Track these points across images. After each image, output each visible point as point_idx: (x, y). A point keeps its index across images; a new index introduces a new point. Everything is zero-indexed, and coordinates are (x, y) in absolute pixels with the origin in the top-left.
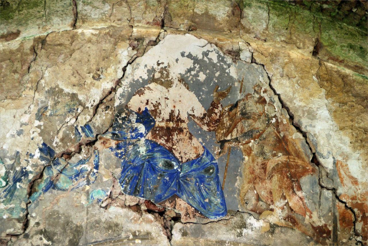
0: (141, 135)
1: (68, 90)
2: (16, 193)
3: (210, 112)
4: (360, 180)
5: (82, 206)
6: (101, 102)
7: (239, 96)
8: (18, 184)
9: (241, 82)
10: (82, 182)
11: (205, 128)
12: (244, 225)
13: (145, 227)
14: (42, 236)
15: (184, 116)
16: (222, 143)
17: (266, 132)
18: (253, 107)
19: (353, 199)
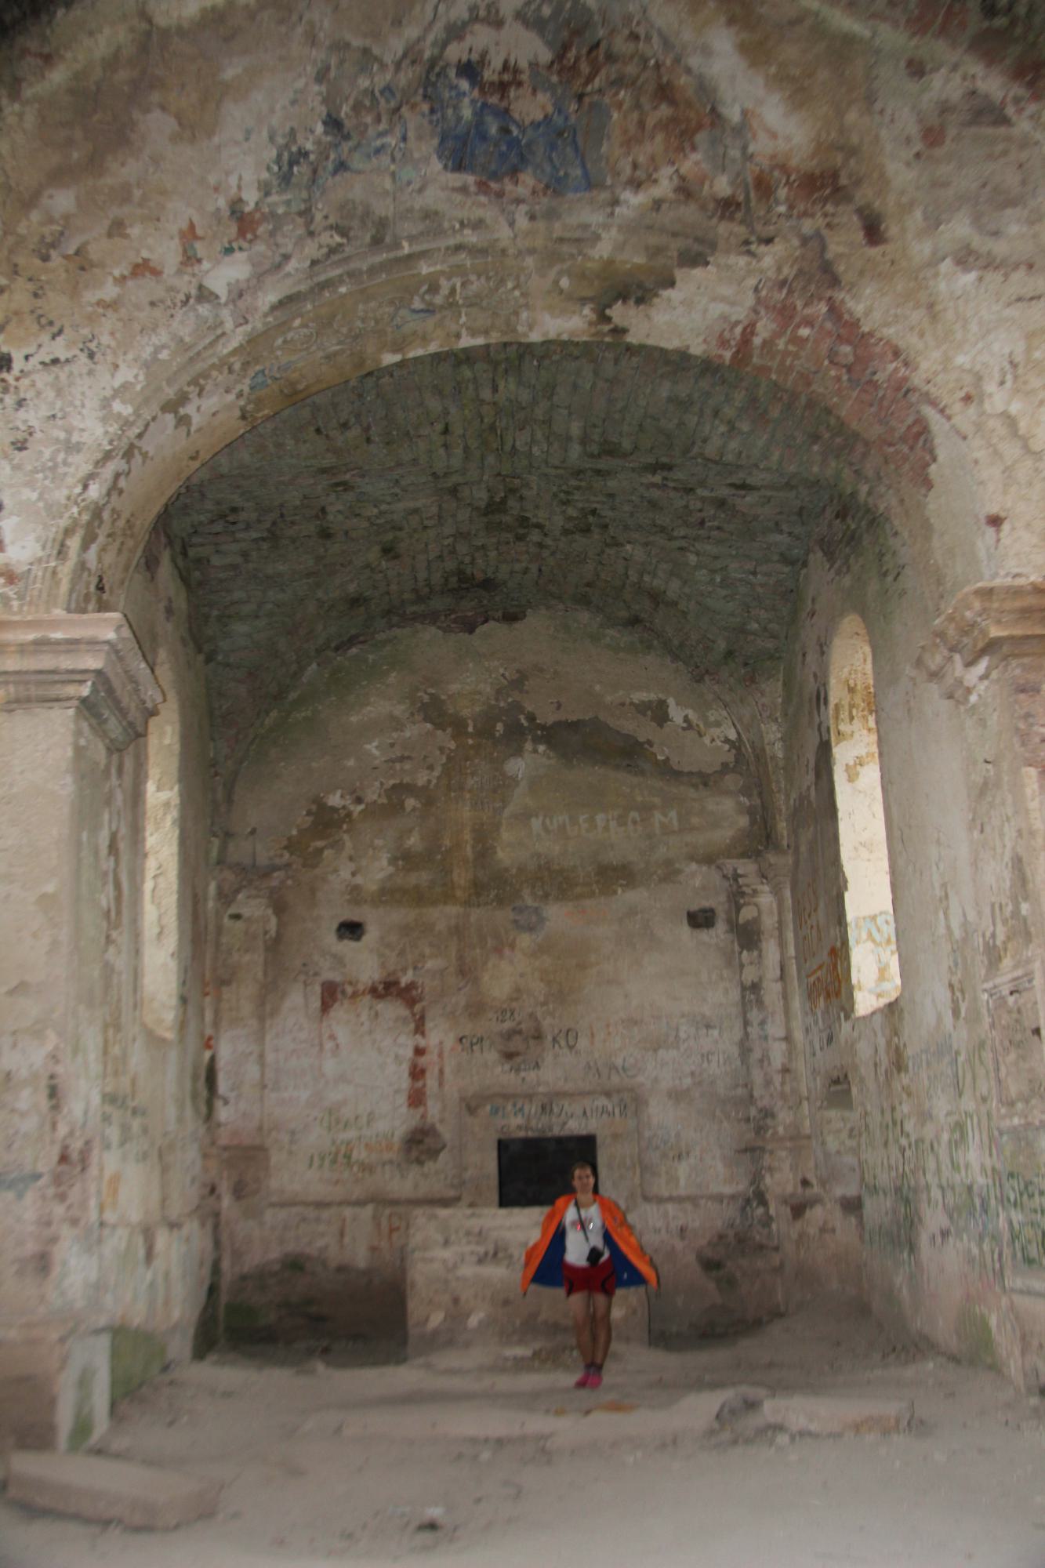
0: (464, 94)
1: (357, 42)
2: (294, 180)
3: (560, 56)
5: (386, 193)
6: (405, 55)
7: (601, 33)
8: (295, 169)
10: (385, 159)
12: (615, 202)
13: (479, 213)
14: (334, 233)
15: (523, 64)
16: (580, 97)
17: (641, 80)
18: (620, 45)
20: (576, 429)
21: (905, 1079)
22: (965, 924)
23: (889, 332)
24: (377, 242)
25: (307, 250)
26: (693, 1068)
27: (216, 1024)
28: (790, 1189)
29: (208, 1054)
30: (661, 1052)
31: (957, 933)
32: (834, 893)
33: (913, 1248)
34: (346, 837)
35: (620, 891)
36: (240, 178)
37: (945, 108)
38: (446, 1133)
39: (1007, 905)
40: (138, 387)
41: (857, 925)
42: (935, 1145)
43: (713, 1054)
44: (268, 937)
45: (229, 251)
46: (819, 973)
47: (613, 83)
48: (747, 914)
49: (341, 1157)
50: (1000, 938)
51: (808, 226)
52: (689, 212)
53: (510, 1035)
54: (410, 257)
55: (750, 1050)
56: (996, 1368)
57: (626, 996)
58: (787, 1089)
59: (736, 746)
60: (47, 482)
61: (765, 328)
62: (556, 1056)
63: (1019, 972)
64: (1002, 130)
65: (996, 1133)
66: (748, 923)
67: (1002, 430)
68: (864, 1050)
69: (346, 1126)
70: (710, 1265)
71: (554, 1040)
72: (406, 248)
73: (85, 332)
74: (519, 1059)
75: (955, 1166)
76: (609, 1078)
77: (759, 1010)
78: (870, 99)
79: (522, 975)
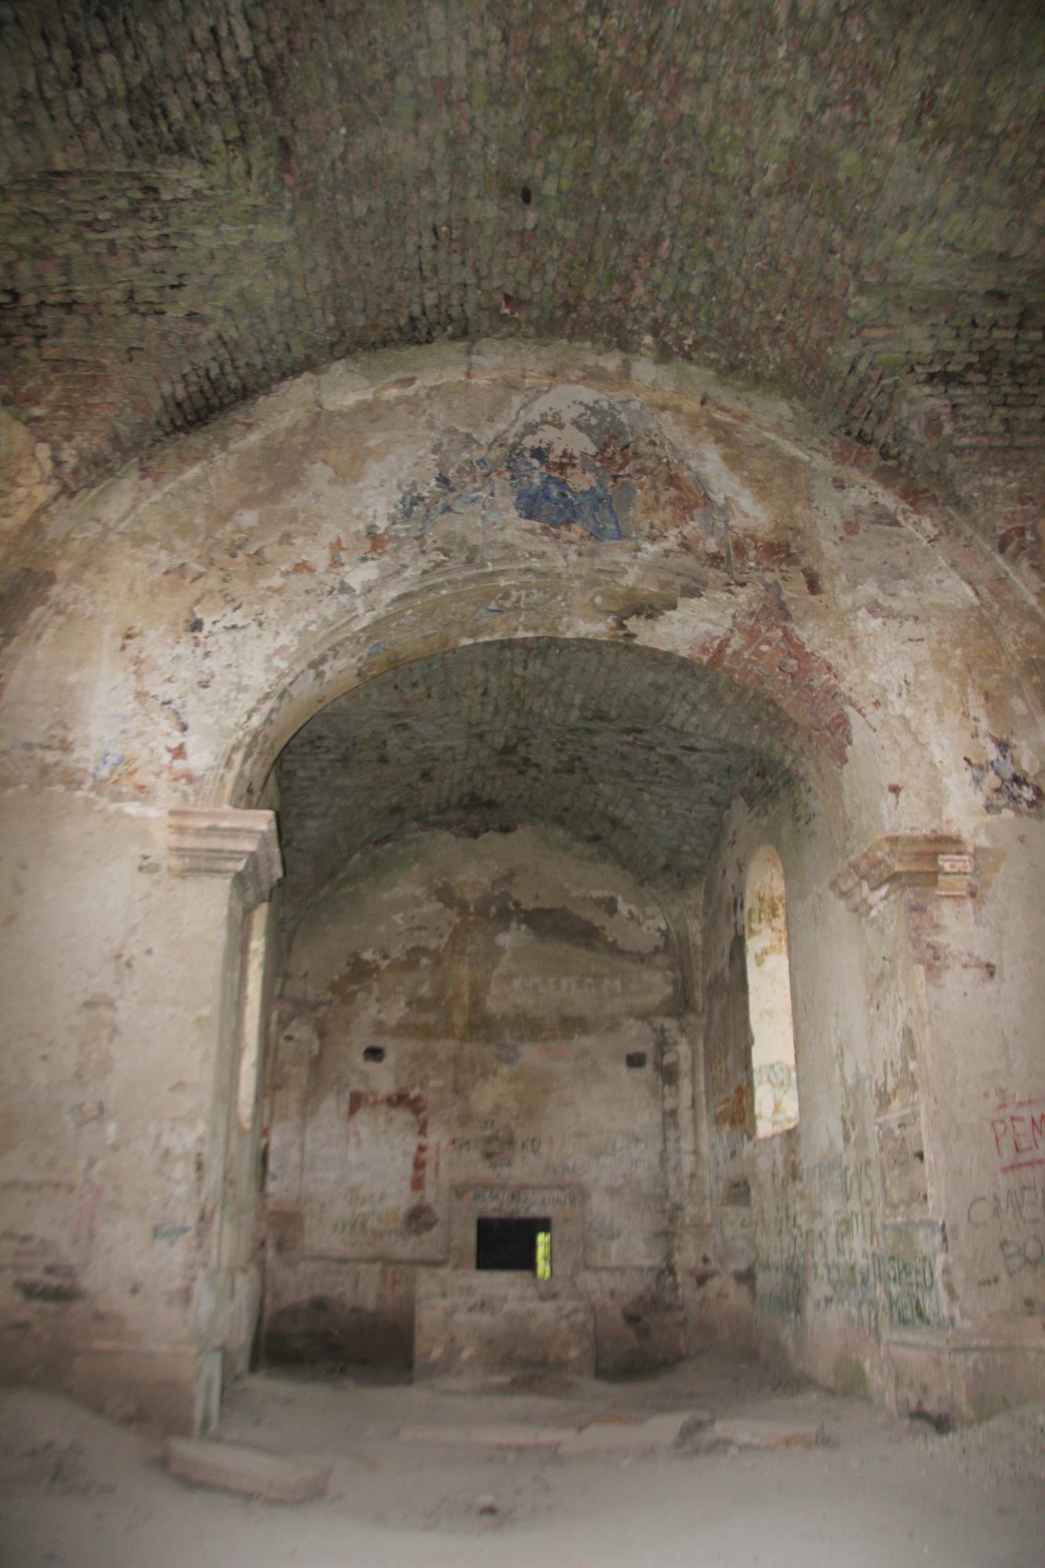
0: (535, 468)
1: (462, 430)
2: (413, 515)
3: (602, 451)
4: (751, 515)
6: (495, 441)
7: (630, 438)
9: (632, 427)
10: (478, 507)
11: (598, 464)
12: (638, 549)
13: (543, 548)
15: (577, 453)
16: (615, 478)
18: (644, 448)
19: (745, 530)
20: (578, 699)
21: (799, 1186)
22: (857, 1075)
23: (824, 653)
24: (470, 561)
25: (419, 564)
27: (271, 1118)
28: (692, 1264)
29: (264, 1142)
30: (602, 1158)
31: (850, 1081)
32: (743, 1047)
33: (799, 1310)
34: (375, 984)
36: (376, 511)
37: (858, 511)
38: (439, 1211)
40: (293, 649)
41: (760, 1071)
42: (824, 1236)
45: (364, 559)
47: (638, 471)
48: (669, 1058)
49: (358, 1225)
50: (891, 1085)
51: (769, 577)
52: (688, 561)
54: (492, 573)
58: (694, 1189)
59: (665, 934)
60: (222, 712)
61: (736, 642)
63: (907, 1111)
64: (896, 529)
67: (900, 727)
68: (763, 1164)
71: (523, 1146)
72: (490, 568)
73: (257, 608)
78: (810, 499)
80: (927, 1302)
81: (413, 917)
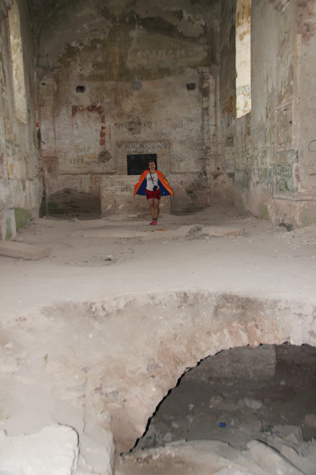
21: (250, 137)
22: (273, 88)
26: (187, 134)
27: (39, 119)
28: (214, 170)
29: (37, 128)
30: (177, 129)
31: (270, 91)
32: (233, 78)
33: (248, 187)
34: (78, 57)
35: (165, 77)
38: (112, 153)
39: (286, 82)
41: (239, 89)
42: (257, 157)
43: (193, 130)
44: (54, 91)
46: (226, 105)
48: (205, 85)
49: (80, 160)
53: (131, 123)
55: (204, 129)
56: (268, 219)
57: (167, 111)
58: (215, 141)
59: (205, 27)
62: (145, 130)
63: (288, 104)
65: (275, 153)
66: (205, 88)
68: (238, 129)
69: (81, 151)
70: (189, 192)
71: (144, 125)
74: (134, 131)
75: (262, 163)
76: (161, 137)
77: (207, 116)
79: (134, 104)
80: (289, 182)
81: (92, 25)
